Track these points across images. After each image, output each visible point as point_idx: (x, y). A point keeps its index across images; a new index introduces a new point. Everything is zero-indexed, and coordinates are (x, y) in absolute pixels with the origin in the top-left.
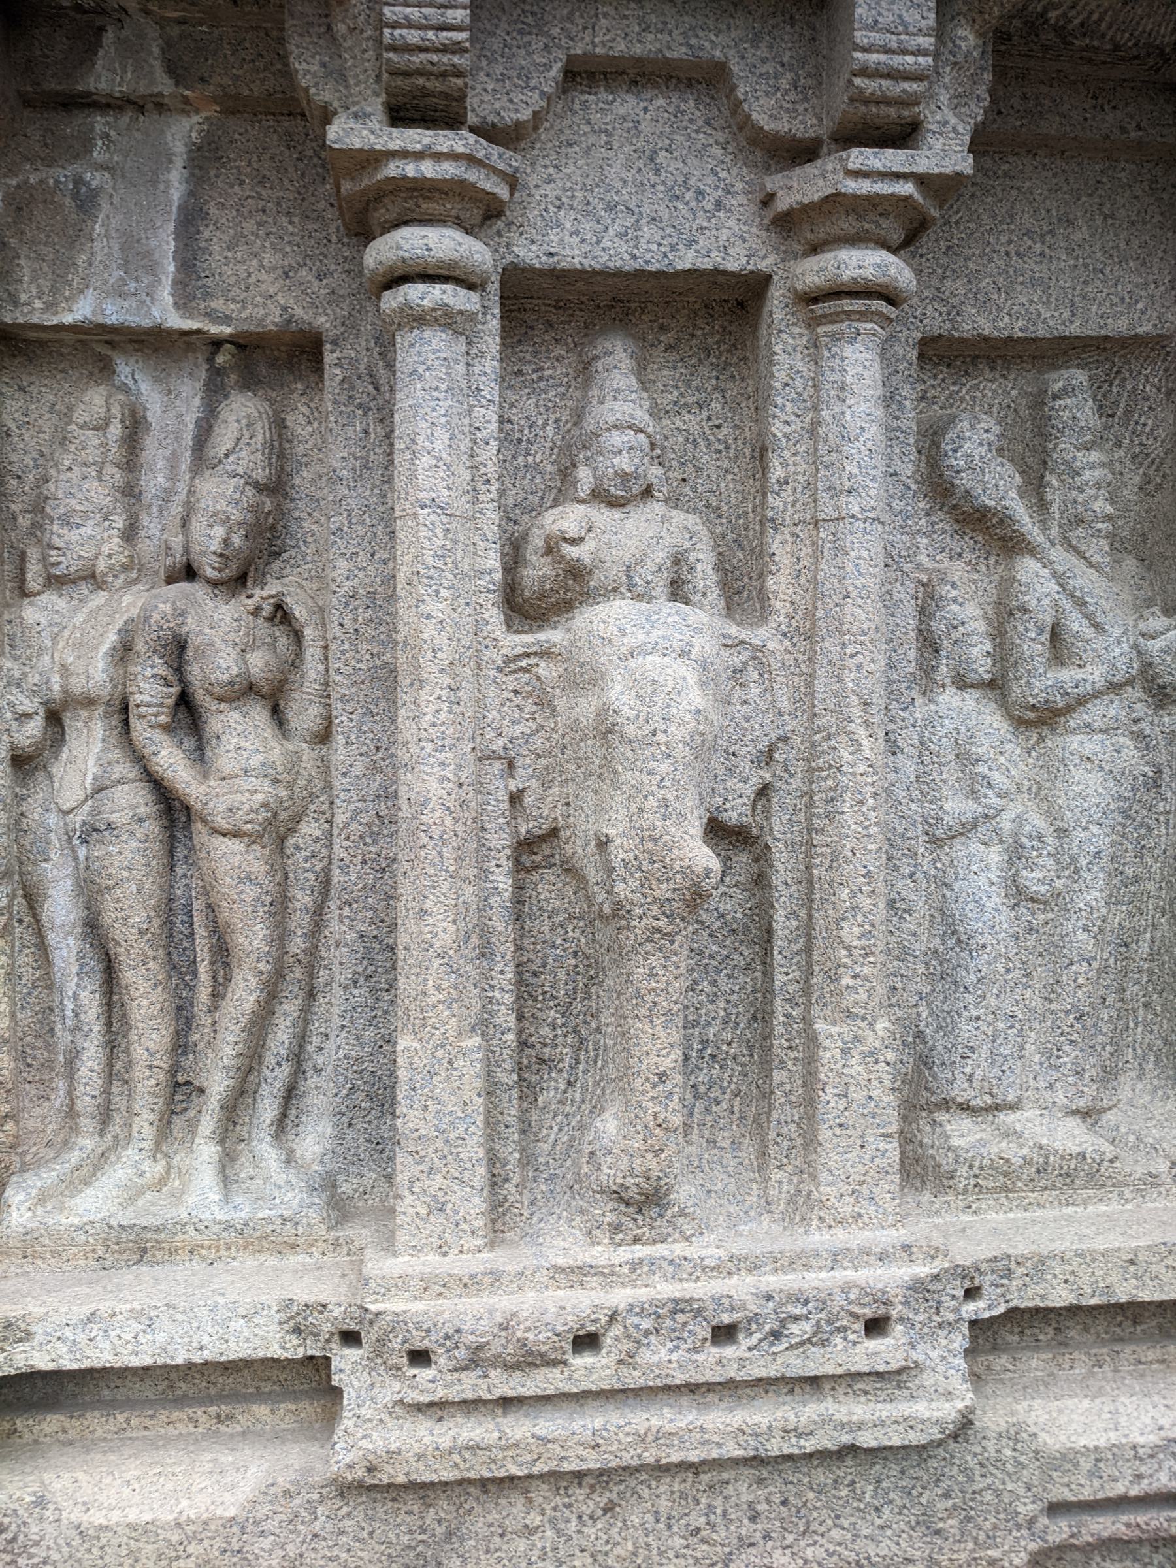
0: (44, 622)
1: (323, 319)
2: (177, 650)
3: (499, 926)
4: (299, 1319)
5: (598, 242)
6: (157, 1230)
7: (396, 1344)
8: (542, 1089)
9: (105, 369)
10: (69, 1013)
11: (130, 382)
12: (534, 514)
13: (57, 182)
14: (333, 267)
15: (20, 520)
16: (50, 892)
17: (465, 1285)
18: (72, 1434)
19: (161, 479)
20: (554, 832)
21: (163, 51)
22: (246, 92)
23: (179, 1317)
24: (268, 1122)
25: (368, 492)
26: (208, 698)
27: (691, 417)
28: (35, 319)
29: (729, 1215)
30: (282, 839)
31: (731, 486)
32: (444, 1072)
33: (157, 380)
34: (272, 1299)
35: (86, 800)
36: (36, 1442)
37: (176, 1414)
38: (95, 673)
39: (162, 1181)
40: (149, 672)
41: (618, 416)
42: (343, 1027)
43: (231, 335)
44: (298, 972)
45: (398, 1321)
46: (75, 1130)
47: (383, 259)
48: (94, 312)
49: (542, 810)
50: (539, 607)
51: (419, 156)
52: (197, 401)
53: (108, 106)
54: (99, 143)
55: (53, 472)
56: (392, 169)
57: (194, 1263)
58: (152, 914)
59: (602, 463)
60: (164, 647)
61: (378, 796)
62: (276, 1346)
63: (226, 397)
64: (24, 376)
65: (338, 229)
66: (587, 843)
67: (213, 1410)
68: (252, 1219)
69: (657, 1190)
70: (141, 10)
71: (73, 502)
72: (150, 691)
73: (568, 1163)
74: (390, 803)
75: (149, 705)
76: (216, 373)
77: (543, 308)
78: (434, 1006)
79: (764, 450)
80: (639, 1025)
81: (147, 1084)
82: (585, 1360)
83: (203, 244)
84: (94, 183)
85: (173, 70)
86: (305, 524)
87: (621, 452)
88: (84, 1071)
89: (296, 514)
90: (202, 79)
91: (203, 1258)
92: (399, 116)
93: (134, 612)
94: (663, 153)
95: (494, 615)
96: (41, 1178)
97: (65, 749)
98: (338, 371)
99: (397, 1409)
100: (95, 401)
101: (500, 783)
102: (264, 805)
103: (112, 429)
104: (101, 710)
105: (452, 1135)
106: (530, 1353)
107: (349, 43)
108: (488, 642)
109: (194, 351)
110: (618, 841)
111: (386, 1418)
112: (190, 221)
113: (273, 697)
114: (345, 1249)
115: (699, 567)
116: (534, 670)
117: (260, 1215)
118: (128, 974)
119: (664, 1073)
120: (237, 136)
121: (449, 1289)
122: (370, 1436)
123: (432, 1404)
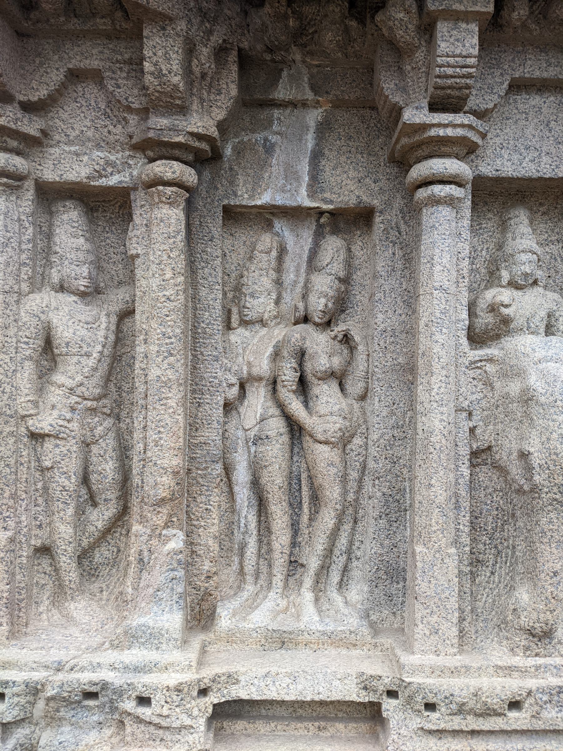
0: (239, 341)
1: (376, 201)
2: (301, 355)
3: (463, 493)
4: (367, 682)
5: (521, 164)
6: (290, 633)
7: (419, 699)
8: (478, 575)
9: (269, 225)
10: (242, 525)
11: (280, 231)
12: (475, 292)
13: (256, 140)
14: (381, 177)
15: (228, 295)
16: (237, 467)
17: (452, 672)
18: (249, 731)
20: (489, 448)
21: (309, 80)
22: (347, 98)
23: (309, 677)
24: (336, 583)
25: (394, 282)
26: (313, 378)
27: (554, 246)
28: (244, 203)
30: (345, 446)
32: (437, 563)
33: (292, 230)
34: (353, 671)
36: (232, 734)
37: (299, 725)
38: (263, 367)
39: (287, 609)
40: (289, 366)
41: (525, 246)
42: (374, 538)
44: (350, 511)
45: (420, 688)
46: (243, 581)
47: (422, 174)
48: (271, 199)
49: (486, 436)
50: (483, 337)
51: (446, 126)
53: (281, 105)
54: (276, 122)
55: (246, 273)
56: (433, 132)
57: (307, 650)
59: (515, 268)
62: (355, 695)
63: (324, 238)
67: (317, 724)
68: (335, 631)
69: (551, 630)
70: (302, 61)
71: (256, 287)
72: (289, 375)
73: (494, 613)
74: (399, 430)
75: (288, 381)
76: (320, 227)
77: (483, 195)
78: (435, 532)
80: (543, 547)
81: (280, 561)
82: (513, 714)
83: (321, 168)
84: (273, 141)
85: (313, 88)
86: (358, 297)
87: (525, 264)
89: (354, 292)
90: (327, 92)
91: (311, 648)
92: (434, 108)
93: (280, 338)
94: (553, 122)
95: (464, 341)
98: (382, 225)
99: (419, 732)
100: (266, 240)
101: (465, 423)
102: (340, 429)
103: (272, 253)
104: (264, 383)
105: (443, 596)
106: (489, 709)
108: (461, 354)
109: (311, 217)
110: (536, 455)
111: (414, 736)
112: (316, 157)
113: (340, 378)
114: (380, 648)
116: (484, 368)
117: (339, 629)
118: (273, 507)
119: (557, 572)
121: (444, 673)
122: (406, 744)
123: (438, 731)
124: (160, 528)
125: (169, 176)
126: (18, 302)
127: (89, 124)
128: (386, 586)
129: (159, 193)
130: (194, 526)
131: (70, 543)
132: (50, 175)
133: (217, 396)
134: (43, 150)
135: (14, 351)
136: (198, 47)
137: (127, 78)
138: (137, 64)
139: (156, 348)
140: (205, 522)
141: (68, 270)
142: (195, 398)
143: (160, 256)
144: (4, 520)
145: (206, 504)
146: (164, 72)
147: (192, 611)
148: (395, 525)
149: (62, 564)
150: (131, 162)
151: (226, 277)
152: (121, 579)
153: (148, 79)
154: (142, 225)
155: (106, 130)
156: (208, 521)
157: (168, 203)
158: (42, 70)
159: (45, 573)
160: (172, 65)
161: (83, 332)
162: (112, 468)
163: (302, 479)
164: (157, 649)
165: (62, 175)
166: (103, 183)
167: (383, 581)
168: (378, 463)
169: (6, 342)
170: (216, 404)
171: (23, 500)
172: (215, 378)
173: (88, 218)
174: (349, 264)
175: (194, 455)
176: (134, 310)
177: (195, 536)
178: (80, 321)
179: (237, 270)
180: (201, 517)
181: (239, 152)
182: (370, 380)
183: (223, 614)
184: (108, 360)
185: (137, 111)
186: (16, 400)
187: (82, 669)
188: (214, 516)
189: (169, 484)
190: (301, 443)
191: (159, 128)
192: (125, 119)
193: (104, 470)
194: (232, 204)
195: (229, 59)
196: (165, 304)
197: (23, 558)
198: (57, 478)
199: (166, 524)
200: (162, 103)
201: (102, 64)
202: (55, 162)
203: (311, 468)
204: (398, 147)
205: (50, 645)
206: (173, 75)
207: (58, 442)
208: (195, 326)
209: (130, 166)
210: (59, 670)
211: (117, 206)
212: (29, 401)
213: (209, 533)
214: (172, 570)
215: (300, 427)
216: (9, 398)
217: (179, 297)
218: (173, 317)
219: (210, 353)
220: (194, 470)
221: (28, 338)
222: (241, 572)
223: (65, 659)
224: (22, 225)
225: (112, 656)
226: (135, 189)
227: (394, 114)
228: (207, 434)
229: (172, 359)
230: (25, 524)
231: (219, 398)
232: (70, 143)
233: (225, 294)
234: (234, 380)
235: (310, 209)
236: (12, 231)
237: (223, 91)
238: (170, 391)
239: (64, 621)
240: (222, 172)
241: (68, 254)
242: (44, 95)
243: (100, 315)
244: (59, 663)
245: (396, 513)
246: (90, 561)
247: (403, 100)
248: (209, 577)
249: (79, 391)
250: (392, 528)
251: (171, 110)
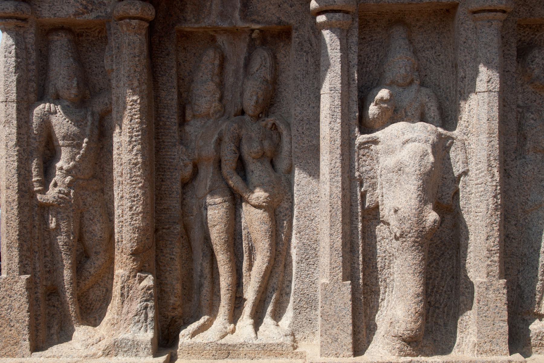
8: (372, 302)
15: (183, 94)
29: (443, 349)
31: (444, 77)
63: (256, 48)
66: (390, 210)
74: (314, 195)
79: (456, 66)
88: (204, 291)
98: (297, 39)
114: (300, 356)
115: (432, 108)
141: (62, 83)
142: (159, 175)
144: (24, 266)
151: (181, 81)
162: (100, 228)
164: (136, 355)
165: (55, 14)
166: (85, 18)
167: (304, 309)
193: (94, 230)
202: (50, 5)
213: (174, 276)
216: (24, 178)
219: (169, 140)
230: (39, 269)
243: (87, 115)
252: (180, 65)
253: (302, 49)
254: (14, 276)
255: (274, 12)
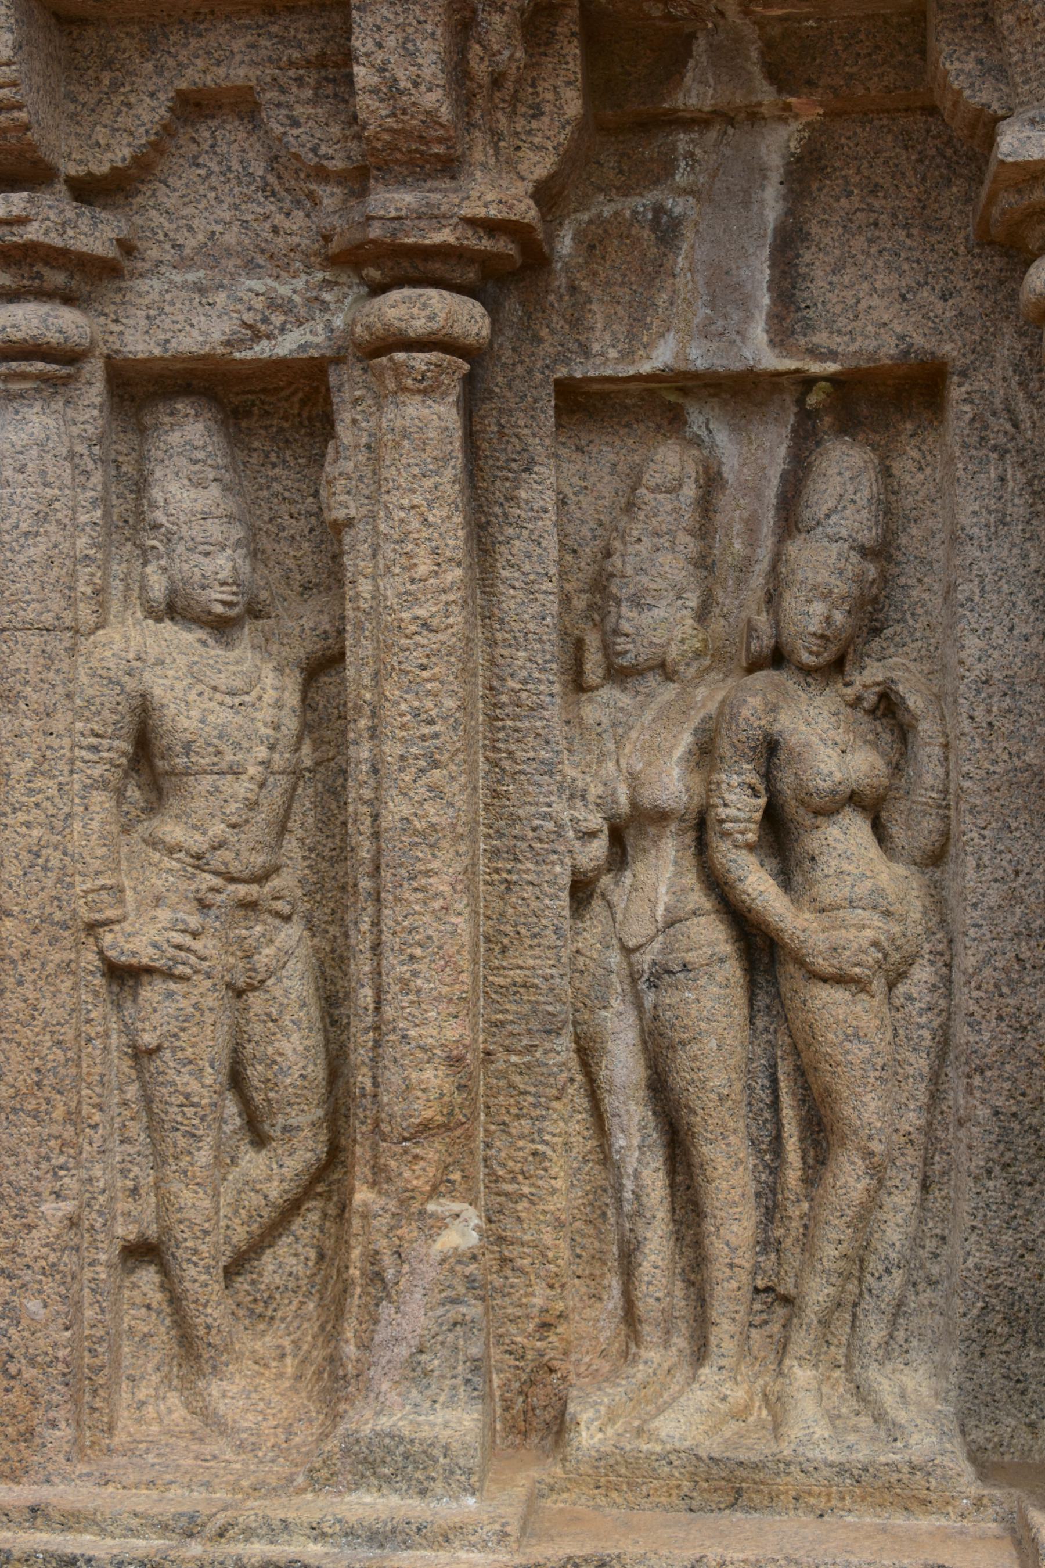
0: (606, 721)
1: (948, 347)
6: (756, 1467)
10: (628, 1195)
11: (703, 433)
13: (635, 212)
14: (961, 284)
15: (575, 601)
16: (610, 1046)
19: (738, 546)
21: (762, 53)
24: (874, 1344)
25: (1005, 553)
26: (802, 811)
28: (608, 372)
33: (735, 429)
35: (656, 935)
38: (671, 784)
40: (735, 780)
42: (973, 1228)
43: (841, 373)
48: (676, 357)
52: (783, 451)
54: (683, 164)
55: (617, 544)
57: (800, 1513)
58: (734, 1076)
60: (753, 749)
61: (1018, 934)
63: (818, 444)
64: (582, 435)
65: (967, 238)
68: (872, 1463)
74: (1033, 943)
76: (806, 416)
86: (914, 593)
88: (646, 1267)
89: (902, 580)
90: (809, 83)
91: (811, 1509)
93: (712, 707)
96: (608, 1395)
97: (628, 873)
98: (967, 408)
100: (669, 460)
107: (1017, 35)
112: (788, 244)
113: (872, 807)
117: (883, 1459)
120: (843, 141)
124: (420, 1198)
125: (419, 326)
126: (72, 651)
127: (227, 216)
128: (1007, 1353)
129: (398, 370)
130: (507, 1195)
131: (206, 1233)
132: (139, 343)
133: (553, 863)
134: (123, 285)
135: (66, 768)
136: (481, 15)
137: (314, 102)
138: (336, 65)
139: (399, 750)
140: (533, 1185)
141: (186, 567)
142: (497, 871)
143: (402, 521)
144: (55, 1174)
145: (533, 1141)
146: (402, 85)
147: (507, 1409)
148: (1029, 1193)
149: (187, 1285)
150: (327, 297)
151: (569, 558)
152: (329, 1327)
153: (365, 103)
154: (357, 446)
155: (267, 225)
156: (540, 1183)
157: (419, 391)
158: (117, 100)
159: (148, 1307)
160: (420, 66)
161: (223, 716)
162: (300, 1048)
163: (781, 1077)
165: (167, 341)
166: (263, 351)
168: (979, 1032)
169: (49, 747)
170: (552, 883)
171: (95, 1127)
172: (547, 816)
173: (227, 435)
174: (888, 510)
175: (500, 1016)
176: (342, 655)
177: (509, 1222)
178: (215, 689)
179: (595, 538)
180: (522, 1172)
181: (591, 245)
182: (952, 813)
183: (584, 1417)
184: (284, 782)
185: (340, 178)
186: (72, 885)
187: (249, 1534)
188: (554, 1171)
189: (440, 1087)
190: (775, 982)
191: (393, 214)
192: (311, 195)
193: (281, 1054)
194: (578, 375)
195: (559, 29)
196: (417, 638)
197: (99, 1269)
198: (172, 1075)
199: (434, 1188)
200: (398, 156)
201: (255, 73)
202: (152, 312)
203: (801, 1046)
204: (995, 212)
205: (169, 1477)
206: (423, 88)
207: (172, 986)
208: (492, 688)
209: (325, 307)
210: (191, 1535)
211: (295, 399)
212: (103, 887)
214: (455, 1301)
215: (772, 940)
216: (59, 881)
217: (451, 620)
218: (436, 670)
219: (531, 755)
220: (501, 1055)
221: (97, 736)
222: (630, 1316)
223: (205, 1510)
224: (77, 467)
225: (314, 1506)
226: (338, 360)
227: (981, 131)
228: (531, 962)
229: (437, 773)
230: (101, 1184)
231: (558, 869)
232: (184, 263)
233: (566, 600)
234: (595, 820)
235: (778, 374)
236: (58, 483)
237: (547, 108)
238: (434, 856)
239: (196, 1424)
240: (552, 297)
241: (184, 528)
242: (124, 159)
244: (192, 1518)
245: (1030, 1160)
246: (253, 1282)
247: (1000, 99)
248: (546, 1326)
249: (216, 860)
250: (1021, 1201)
251: (422, 167)
252: (564, 503)
253: (982, 438)
254: (22, 1208)
255: (886, 318)
